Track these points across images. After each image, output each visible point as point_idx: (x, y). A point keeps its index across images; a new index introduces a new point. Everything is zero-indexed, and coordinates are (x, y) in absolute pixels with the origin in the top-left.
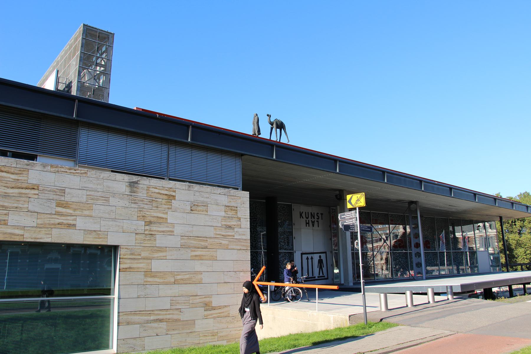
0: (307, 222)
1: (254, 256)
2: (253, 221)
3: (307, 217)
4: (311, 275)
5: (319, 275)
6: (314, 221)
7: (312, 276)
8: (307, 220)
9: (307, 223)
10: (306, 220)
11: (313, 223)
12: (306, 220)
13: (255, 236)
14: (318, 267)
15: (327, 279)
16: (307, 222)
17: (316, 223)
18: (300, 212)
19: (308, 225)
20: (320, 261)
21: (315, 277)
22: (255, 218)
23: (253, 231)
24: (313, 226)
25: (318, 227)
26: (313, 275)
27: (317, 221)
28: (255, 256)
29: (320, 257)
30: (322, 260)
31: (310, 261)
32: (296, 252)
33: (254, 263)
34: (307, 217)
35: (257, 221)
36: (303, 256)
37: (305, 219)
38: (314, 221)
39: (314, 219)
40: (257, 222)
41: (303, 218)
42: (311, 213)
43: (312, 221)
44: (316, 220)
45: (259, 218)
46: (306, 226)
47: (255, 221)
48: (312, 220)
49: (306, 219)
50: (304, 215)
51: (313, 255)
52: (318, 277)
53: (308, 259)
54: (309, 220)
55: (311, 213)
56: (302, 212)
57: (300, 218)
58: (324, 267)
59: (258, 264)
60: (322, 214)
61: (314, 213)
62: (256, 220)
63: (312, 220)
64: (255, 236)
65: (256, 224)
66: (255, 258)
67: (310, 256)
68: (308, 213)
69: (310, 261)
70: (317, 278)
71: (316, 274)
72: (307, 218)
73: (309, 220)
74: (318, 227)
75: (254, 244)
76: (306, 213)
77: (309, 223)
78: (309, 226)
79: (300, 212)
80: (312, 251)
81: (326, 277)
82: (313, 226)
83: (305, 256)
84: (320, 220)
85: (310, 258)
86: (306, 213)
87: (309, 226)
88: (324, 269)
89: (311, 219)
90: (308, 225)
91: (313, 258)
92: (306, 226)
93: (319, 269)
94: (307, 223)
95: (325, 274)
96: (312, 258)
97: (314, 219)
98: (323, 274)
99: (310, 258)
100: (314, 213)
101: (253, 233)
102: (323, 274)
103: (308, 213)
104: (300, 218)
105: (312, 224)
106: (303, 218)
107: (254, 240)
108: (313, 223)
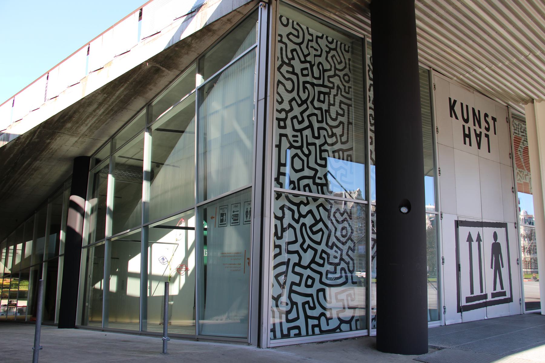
0: (467, 132)
1: (318, 218)
2: (320, 93)
3: (466, 117)
5: (495, 289)
6: (481, 132)
8: (467, 126)
9: (465, 136)
10: (464, 126)
11: (478, 138)
12: (464, 126)
13: (323, 145)
14: (492, 268)
15: (510, 300)
17: (484, 140)
18: (450, 99)
19: (467, 139)
21: (485, 296)
22: (323, 86)
23: (319, 129)
27: (487, 136)
28: (321, 220)
29: (495, 236)
31: (475, 244)
32: (444, 215)
33: (319, 243)
34: (466, 117)
35: (332, 96)
36: (461, 228)
37: (461, 122)
38: (481, 132)
40: (332, 102)
41: (457, 118)
42: (473, 110)
43: (475, 130)
45: (338, 87)
46: (465, 143)
47: (326, 96)
48: (475, 128)
49: (464, 124)
50: (457, 108)
52: (493, 295)
53: (470, 239)
54: (469, 128)
56: (455, 101)
58: (503, 267)
59: (331, 248)
61: (479, 111)
62: (329, 94)
63: (475, 128)
64: (323, 145)
65: (330, 105)
66: (320, 225)
67: (474, 231)
68: (467, 106)
69: (475, 244)
70: (490, 298)
71: (489, 290)
72: (466, 121)
73: (469, 128)
75: (319, 175)
76: (462, 104)
77: (469, 136)
78: (470, 145)
79: (450, 99)
80: (477, 218)
81: (508, 296)
83: (464, 231)
84: (491, 133)
85: (474, 238)
86: (462, 104)
88: (504, 271)
89: (475, 125)
91: (482, 238)
92: (465, 143)
93: (493, 270)
95: (506, 289)
96: (479, 239)
98: (502, 288)
99: (474, 238)
100: (479, 111)
101: (316, 135)
102: (502, 288)
103: (467, 106)
104: (451, 116)
106: (457, 118)
107: (321, 158)
108: (478, 138)
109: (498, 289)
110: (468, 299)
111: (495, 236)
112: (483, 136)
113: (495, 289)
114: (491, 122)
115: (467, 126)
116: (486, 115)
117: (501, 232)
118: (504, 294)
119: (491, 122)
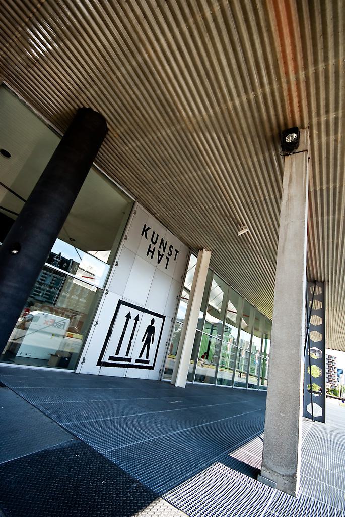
0: (152, 249)
4: (122, 354)
5: (140, 357)
6: (163, 255)
7: (124, 357)
8: (153, 246)
9: (149, 251)
10: (150, 245)
11: (160, 257)
12: (150, 245)
14: (142, 341)
15: (152, 368)
16: (152, 249)
17: (164, 260)
18: (145, 225)
19: (150, 254)
20: (151, 330)
21: (130, 360)
24: (159, 262)
25: (166, 268)
26: (127, 355)
29: (153, 321)
30: (154, 328)
31: (132, 322)
39: (164, 251)
41: (146, 237)
42: (162, 240)
44: (166, 255)
46: (147, 255)
49: (151, 244)
51: (140, 313)
52: (137, 361)
53: (128, 316)
54: (154, 248)
55: (162, 240)
56: (149, 228)
57: (142, 235)
58: (152, 343)
60: (177, 252)
61: (166, 242)
67: (134, 313)
68: (158, 235)
69: (132, 322)
70: (133, 362)
71: (134, 355)
72: (154, 243)
73: (154, 248)
74: (166, 268)
76: (154, 232)
77: (153, 253)
78: (152, 258)
79: (145, 225)
81: (151, 364)
82: (159, 262)
83: (124, 310)
84: (171, 258)
85: (133, 316)
86: (154, 232)
87: (152, 258)
88: (153, 347)
89: (160, 248)
90: (150, 254)
92: (147, 255)
94: (150, 252)
96: (137, 319)
97: (164, 251)
98: (147, 358)
99: (133, 316)
102: (147, 358)
103: (158, 235)
104: (142, 235)
105: (158, 258)
106: (146, 237)
108: (160, 257)
109: (144, 358)
110: (111, 358)
111: (153, 321)
112: (164, 257)
113: (140, 357)
114: (174, 253)
115: (153, 246)
116: (171, 247)
117: (158, 322)
118: (148, 362)
119: (174, 253)
